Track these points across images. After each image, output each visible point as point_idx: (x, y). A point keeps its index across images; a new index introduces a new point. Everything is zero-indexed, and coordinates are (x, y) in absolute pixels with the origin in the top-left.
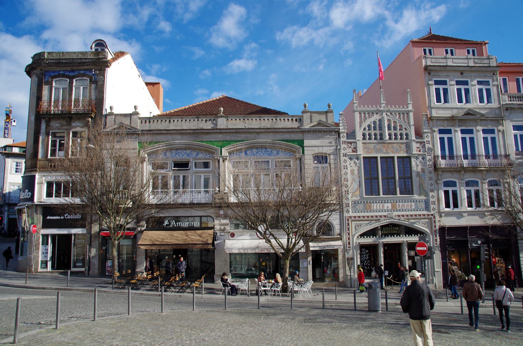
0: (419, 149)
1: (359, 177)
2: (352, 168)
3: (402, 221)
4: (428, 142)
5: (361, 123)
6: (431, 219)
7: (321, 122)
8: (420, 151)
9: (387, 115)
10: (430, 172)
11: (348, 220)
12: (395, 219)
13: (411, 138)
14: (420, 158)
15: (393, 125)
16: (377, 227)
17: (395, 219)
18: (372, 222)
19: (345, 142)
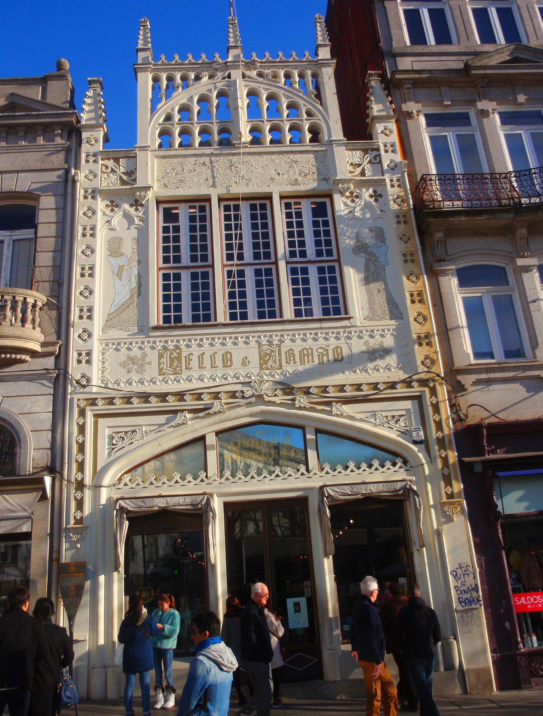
0: (359, 170)
1: (139, 262)
2: (113, 234)
3: (300, 408)
4: (390, 149)
5: (155, 101)
6: (419, 399)
7: (16, 100)
8: (363, 173)
9: (244, 76)
10: (405, 238)
11: (82, 413)
12: (273, 404)
13: (330, 135)
14: (366, 194)
15: (265, 105)
16: (202, 438)
17: (273, 404)
18: (179, 418)
19: (95, 155)
